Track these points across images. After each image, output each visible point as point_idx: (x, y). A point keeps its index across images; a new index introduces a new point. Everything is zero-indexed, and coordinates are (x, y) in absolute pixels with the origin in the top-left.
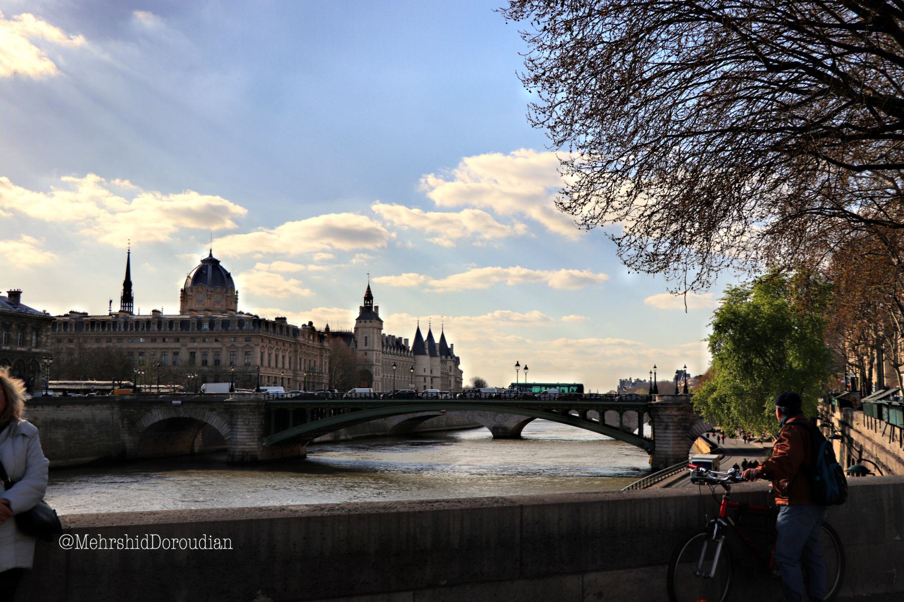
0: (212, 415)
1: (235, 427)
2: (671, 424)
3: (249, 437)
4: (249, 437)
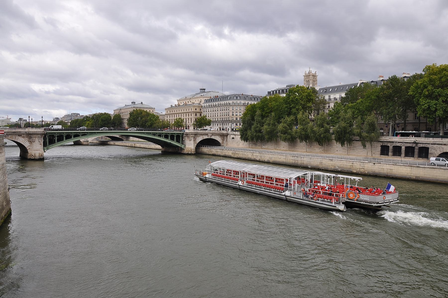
0: (20, 138)
1: (32, 143)
2: (192, 139)
3: (41, 147)
4: (41, 147)
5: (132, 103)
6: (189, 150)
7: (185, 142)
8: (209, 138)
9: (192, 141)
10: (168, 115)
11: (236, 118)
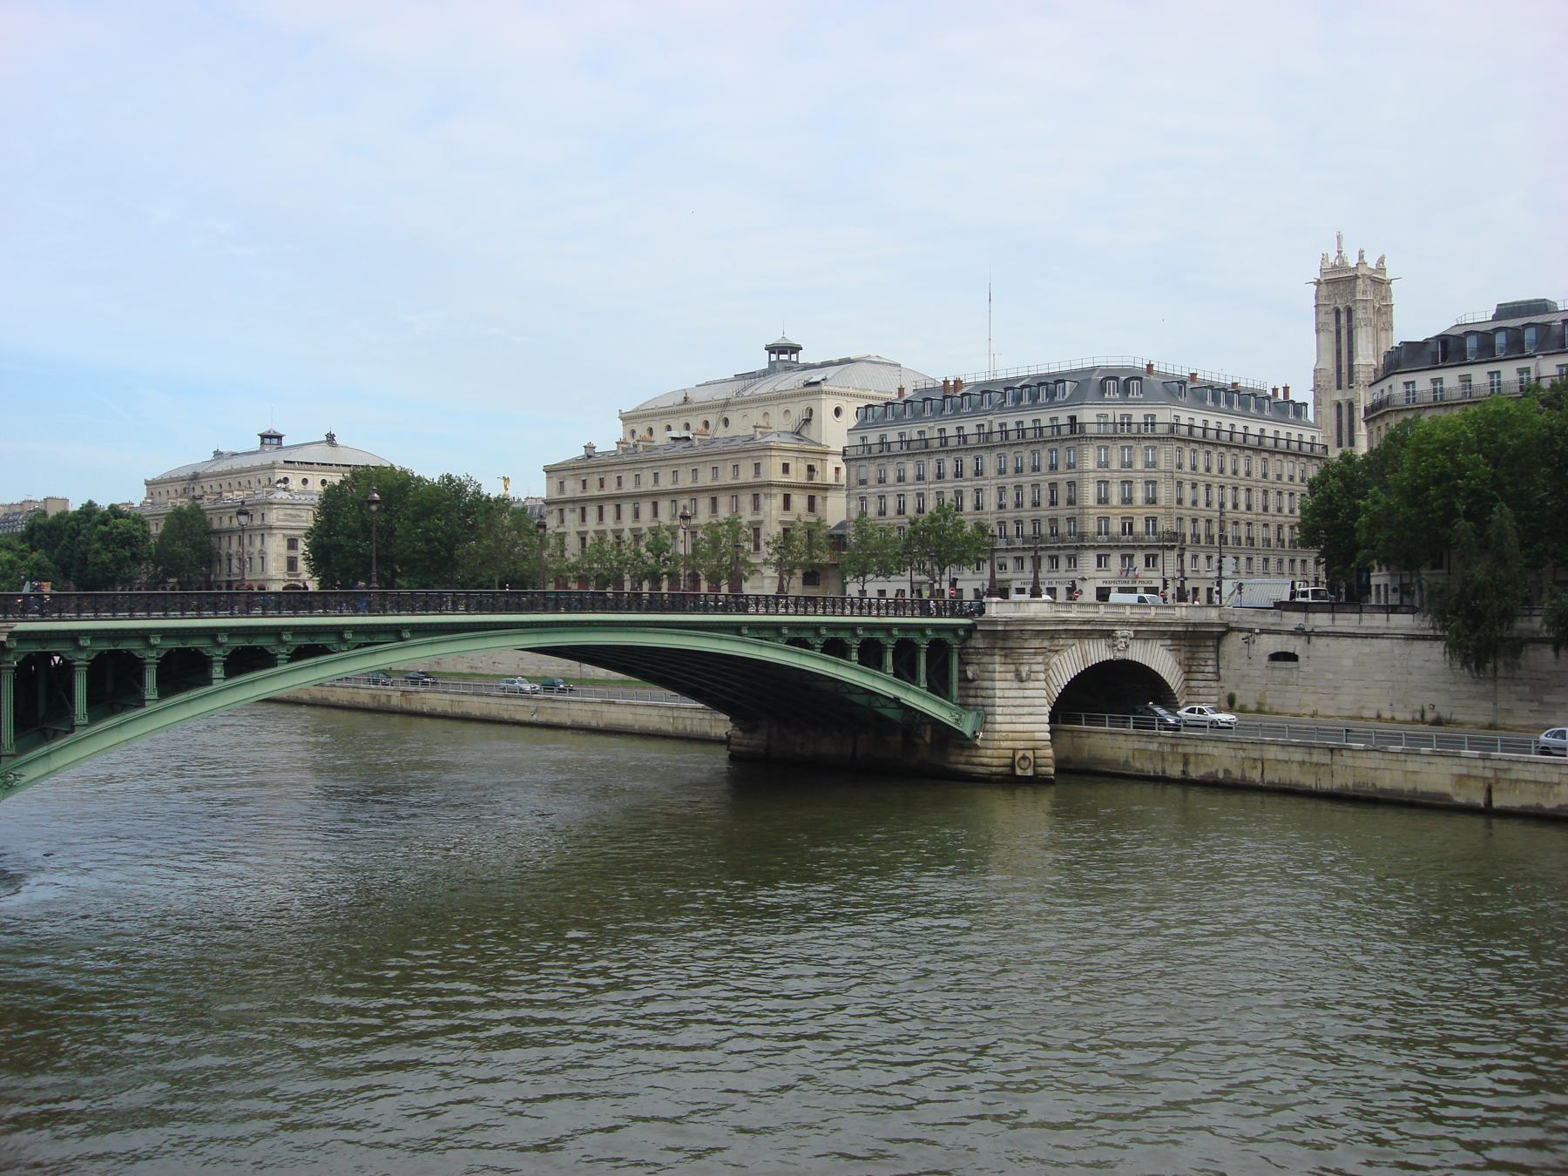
5: (263, 437)
6: (1020, 754)
7: (984, 693)
8: (1120, 655)
9: (1037, 684)
10: (570, 506)
11: (1147, 520)
